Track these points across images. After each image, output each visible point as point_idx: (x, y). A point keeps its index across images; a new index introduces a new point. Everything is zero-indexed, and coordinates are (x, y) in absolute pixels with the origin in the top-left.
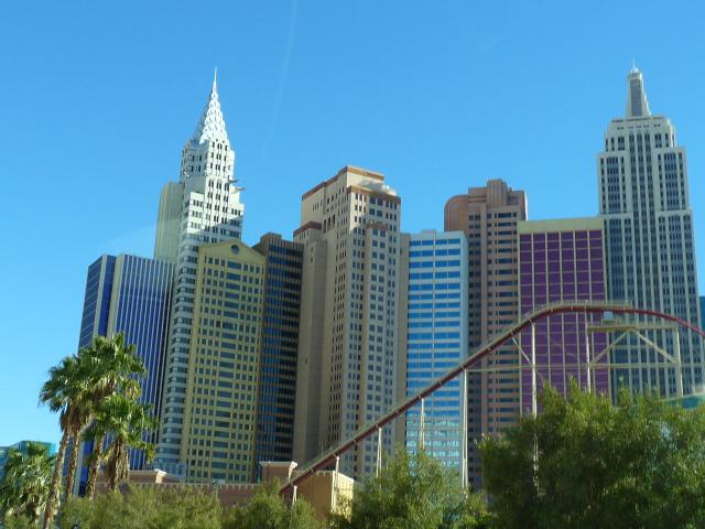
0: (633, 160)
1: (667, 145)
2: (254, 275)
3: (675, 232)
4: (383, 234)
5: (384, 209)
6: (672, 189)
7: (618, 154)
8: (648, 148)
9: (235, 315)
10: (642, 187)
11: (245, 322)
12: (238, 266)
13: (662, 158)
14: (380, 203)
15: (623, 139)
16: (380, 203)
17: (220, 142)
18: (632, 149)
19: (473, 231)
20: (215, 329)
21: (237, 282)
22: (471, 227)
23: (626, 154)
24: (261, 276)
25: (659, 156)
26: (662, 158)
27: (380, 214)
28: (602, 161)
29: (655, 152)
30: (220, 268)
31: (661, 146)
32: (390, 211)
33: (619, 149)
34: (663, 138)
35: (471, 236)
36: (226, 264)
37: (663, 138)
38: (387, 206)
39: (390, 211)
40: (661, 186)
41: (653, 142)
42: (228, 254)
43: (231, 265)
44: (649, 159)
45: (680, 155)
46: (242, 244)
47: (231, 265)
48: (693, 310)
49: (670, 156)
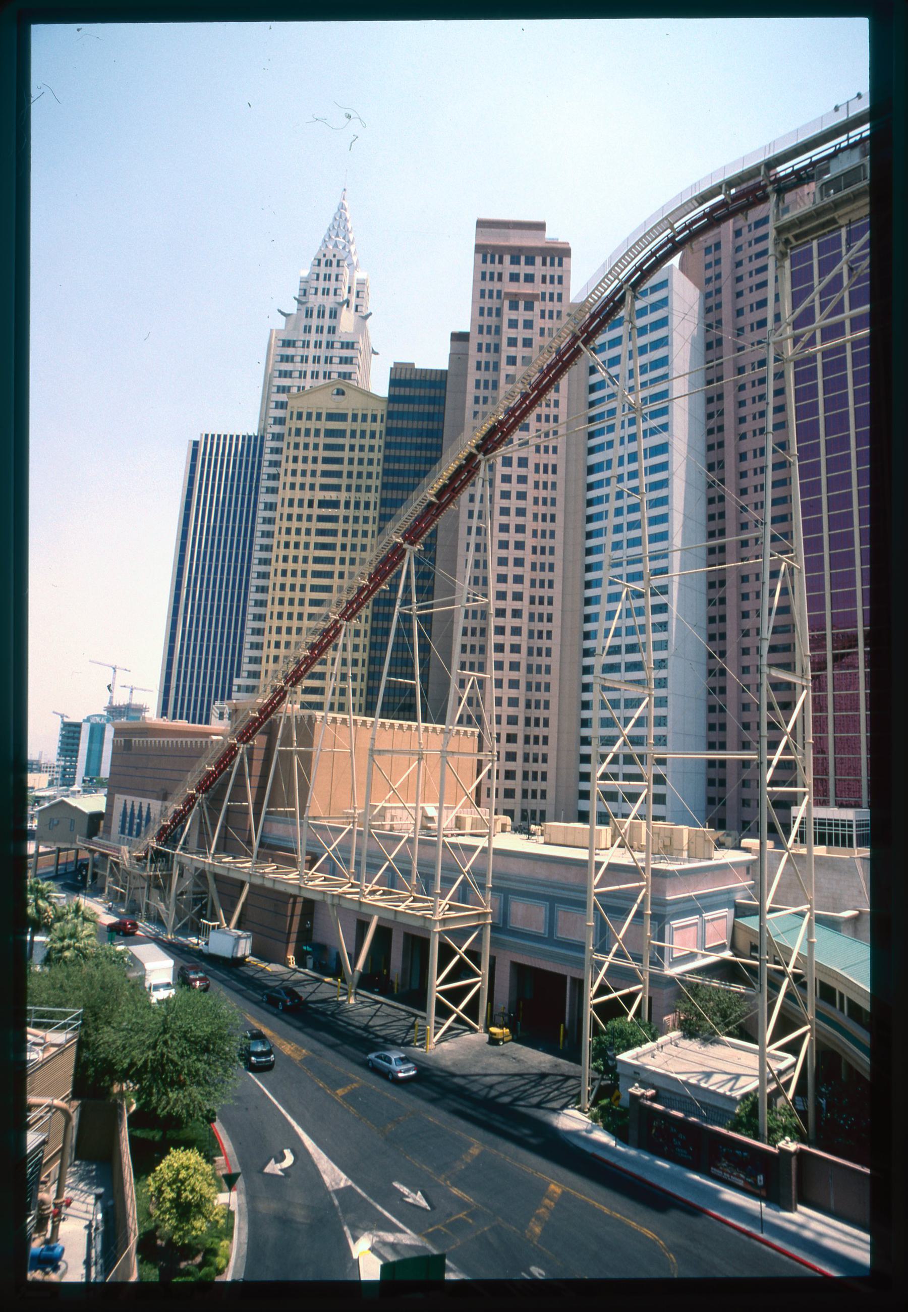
2: (368, 426)
4: (529, 307)
5: (538, 269)
9: (337, 488)
11: (353, 496)
12: (342, 417)
14: (530, 261)
16: (530, 261)
17: (329, 257)
19: (710, 273)
20: (306, 511)
21: (340, 441)
24: (379, 427)
27: (529, 278)
30: (313, 425)
32: (548, 271)
35: (708, 281)
36: (324, 417)
38: (544, 264)
39: (548, 271)
42: (328, 403)
43: (331, 417)
46: (349, 386)
47: (331, 417)
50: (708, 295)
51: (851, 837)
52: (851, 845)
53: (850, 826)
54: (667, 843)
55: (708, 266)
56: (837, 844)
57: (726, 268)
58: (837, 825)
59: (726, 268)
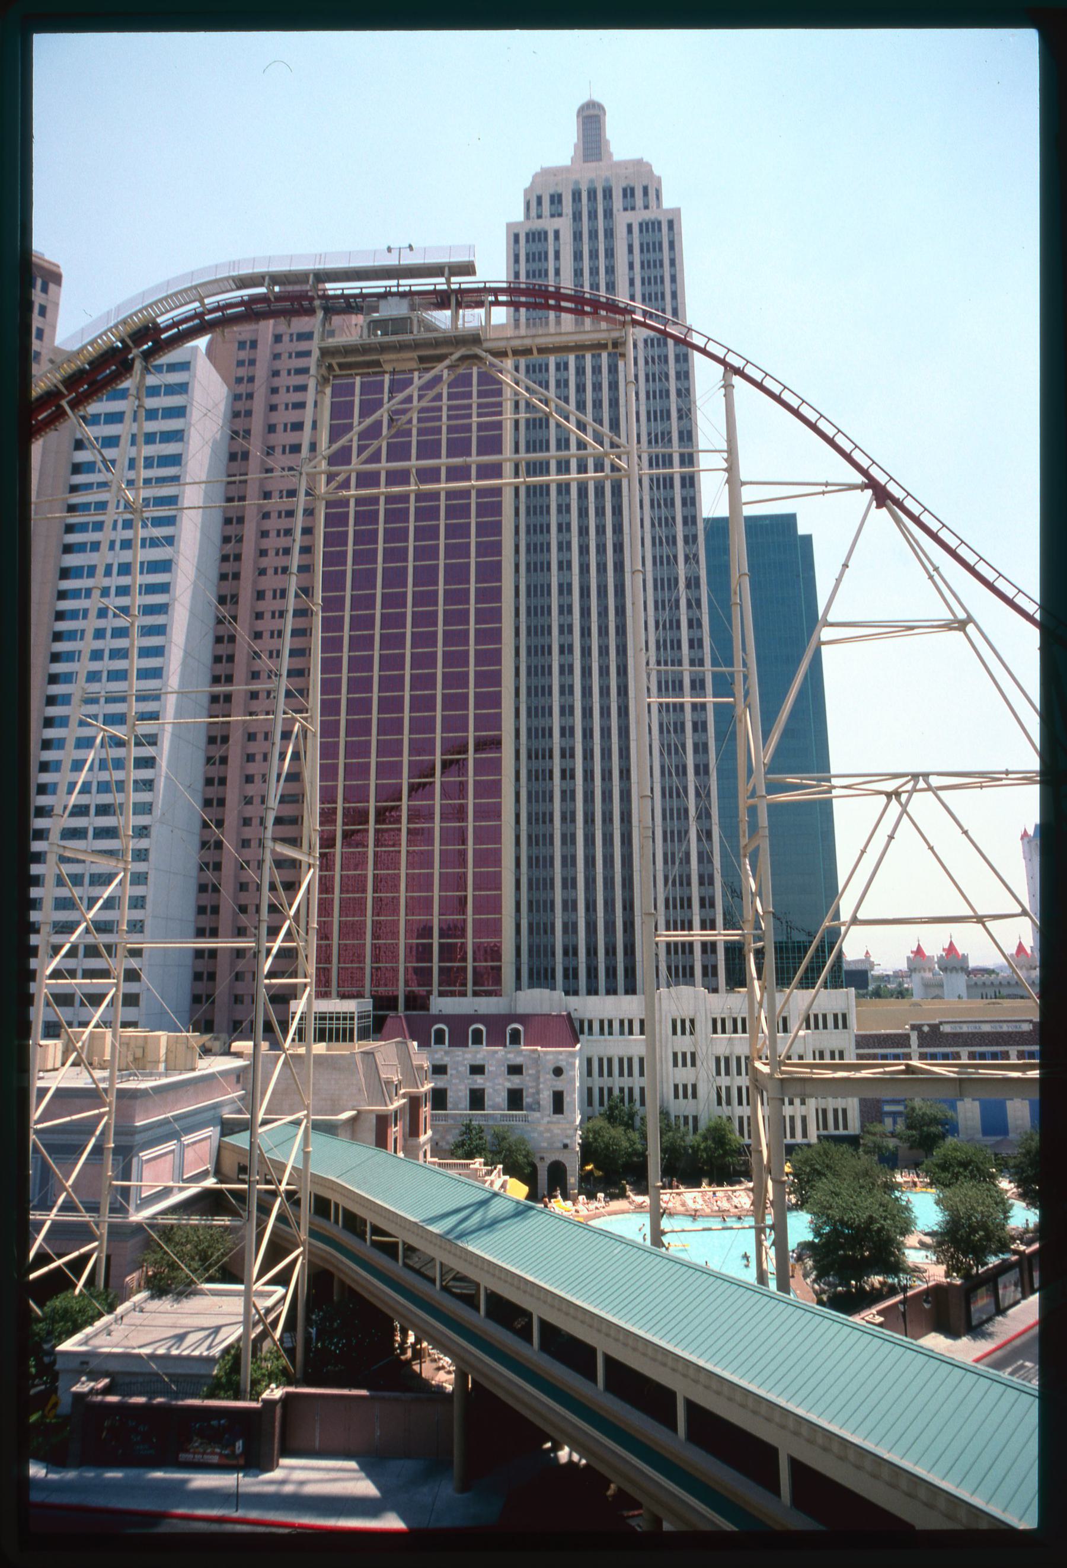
0: (577, 236)
1: (646, 207)
3: (653, 272)
6: (657, 368)
7: (550, 225)
8: (609, 214)
10: (594, 255)
13: (636, 229)
15: (560, 196)
18: (577, 217)
19: (242, 372)
22: (240, 363)
23: (564, 224)
25: (630, 227)
26: (636, 229)
28: (516, 238)
29: (622, 219)
31: (633, 209)
33: (552, 216)
34: (639, 193)
35: (239, 380)
37: (639, 193)
40: (632, 283)
41: (618, 202)
44: (610, 233)
45: (671, 224)
48: (690, 540)
49: (650, 227)
50: (237, 397)
51: (352, 1030)
52: (352, 1040)
53: (352, 1019)
54: (139, 1054)
55: (240, 363)
56: (337, 1040)
57: (261, 372)
58: (338, 1019)
59: (261, 372)
